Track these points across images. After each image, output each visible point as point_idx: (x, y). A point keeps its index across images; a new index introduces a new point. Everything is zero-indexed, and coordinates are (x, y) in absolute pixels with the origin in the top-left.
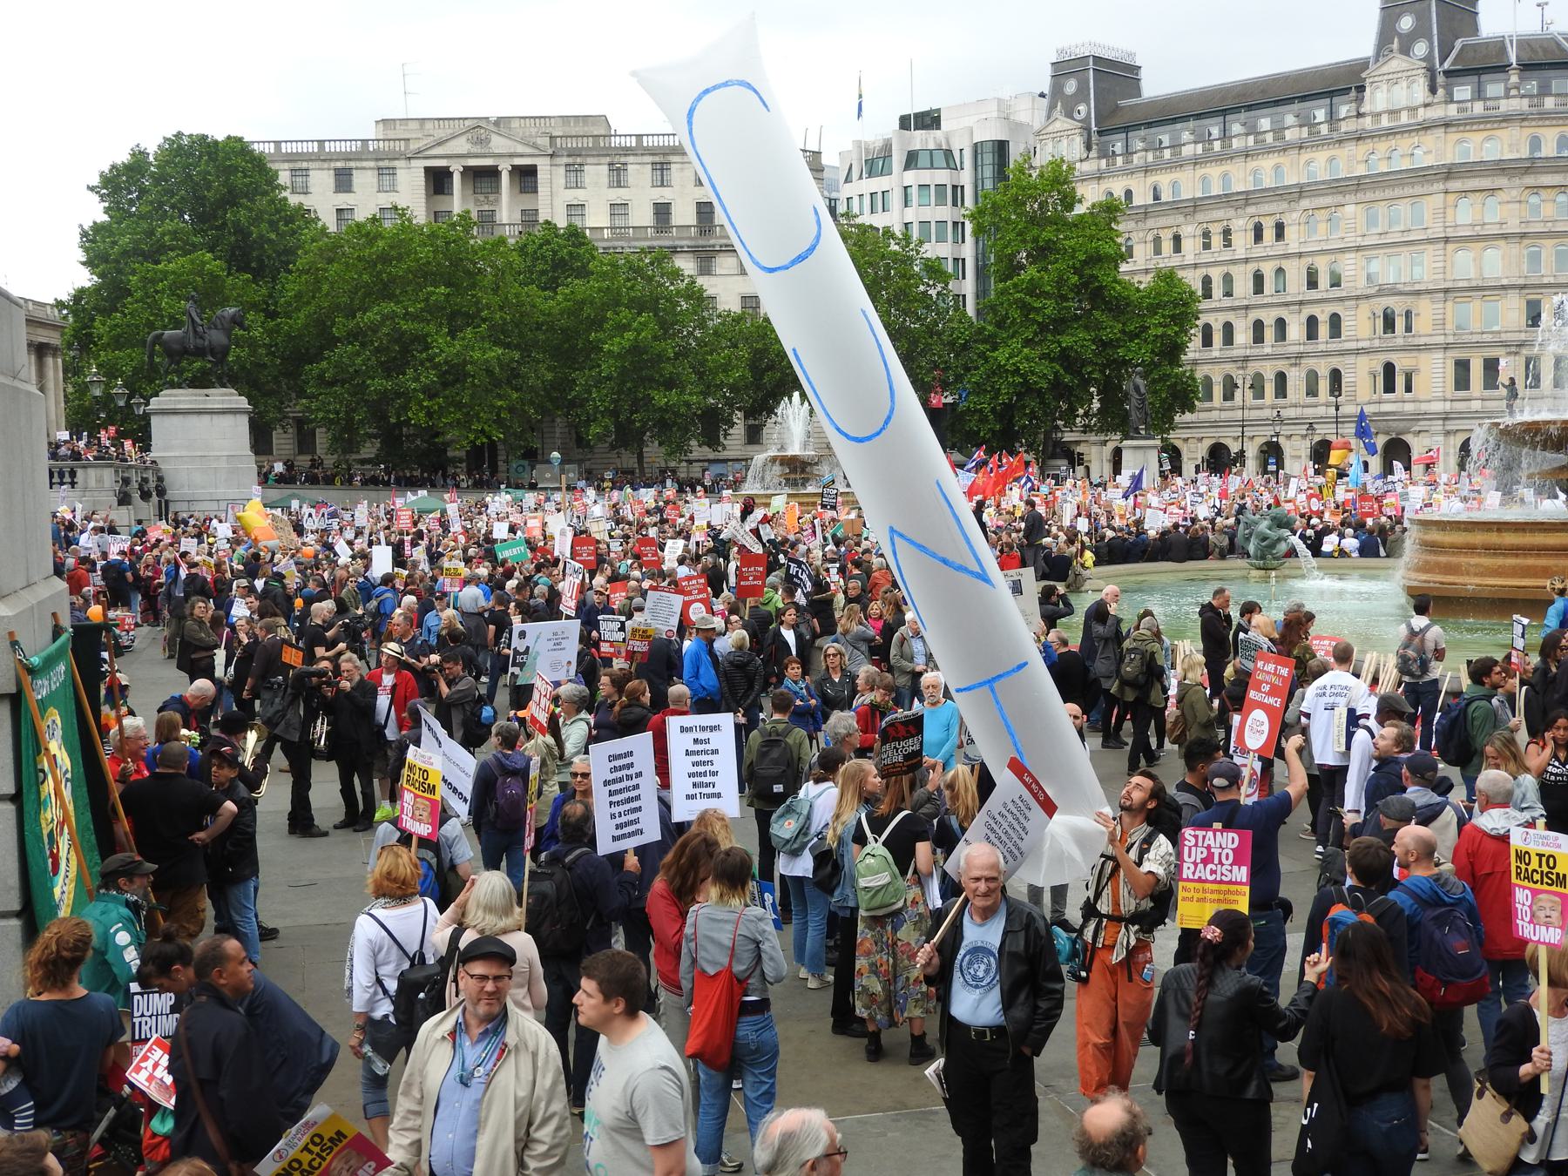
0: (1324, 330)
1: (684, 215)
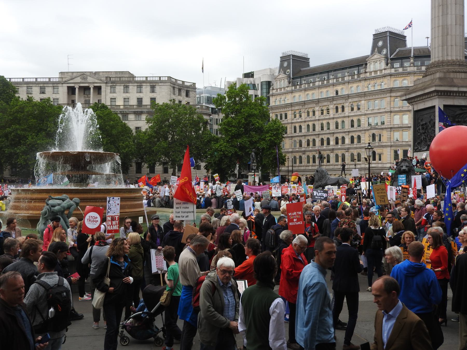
0: (356, 140)
1: (146, 102)
